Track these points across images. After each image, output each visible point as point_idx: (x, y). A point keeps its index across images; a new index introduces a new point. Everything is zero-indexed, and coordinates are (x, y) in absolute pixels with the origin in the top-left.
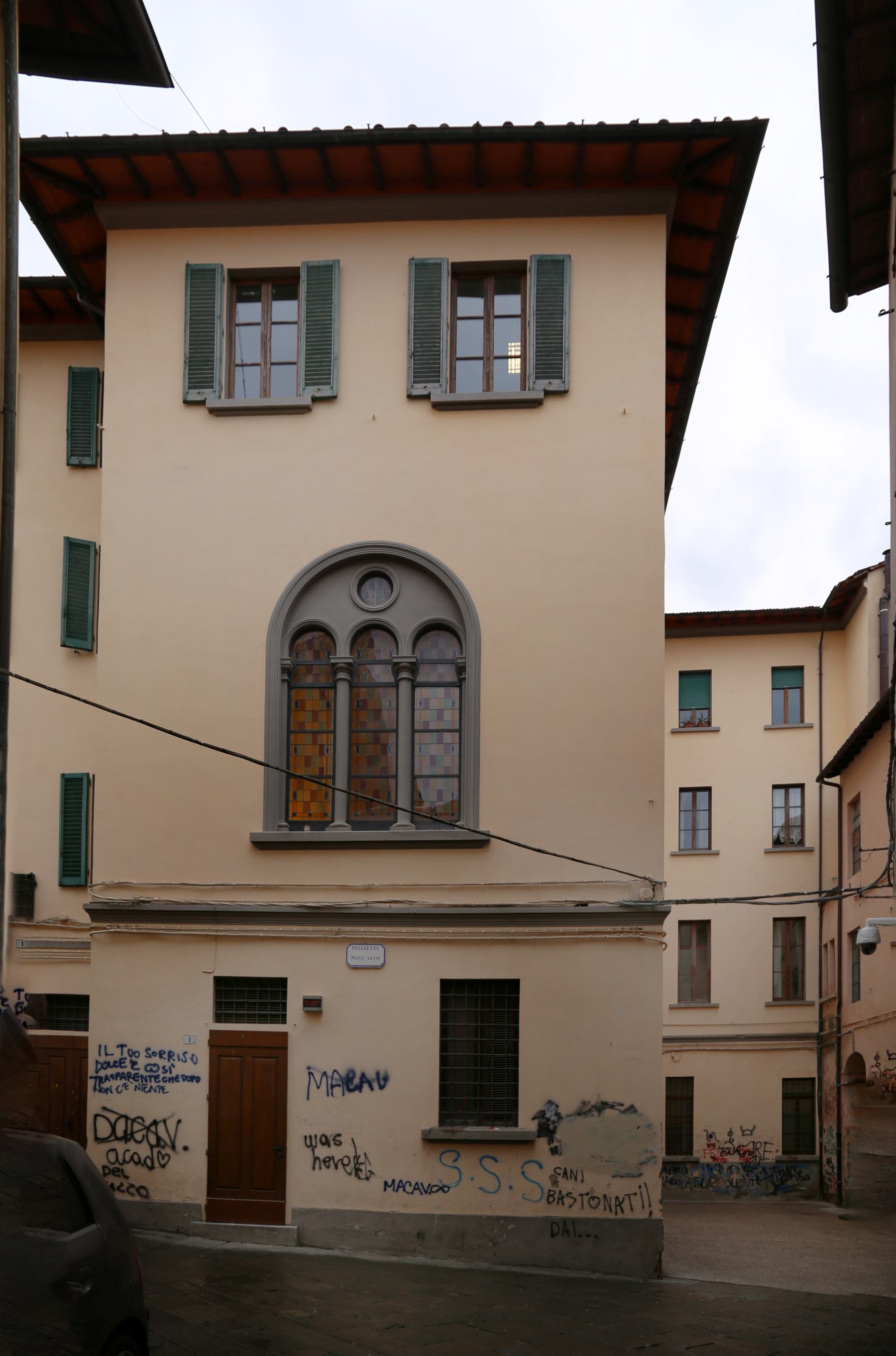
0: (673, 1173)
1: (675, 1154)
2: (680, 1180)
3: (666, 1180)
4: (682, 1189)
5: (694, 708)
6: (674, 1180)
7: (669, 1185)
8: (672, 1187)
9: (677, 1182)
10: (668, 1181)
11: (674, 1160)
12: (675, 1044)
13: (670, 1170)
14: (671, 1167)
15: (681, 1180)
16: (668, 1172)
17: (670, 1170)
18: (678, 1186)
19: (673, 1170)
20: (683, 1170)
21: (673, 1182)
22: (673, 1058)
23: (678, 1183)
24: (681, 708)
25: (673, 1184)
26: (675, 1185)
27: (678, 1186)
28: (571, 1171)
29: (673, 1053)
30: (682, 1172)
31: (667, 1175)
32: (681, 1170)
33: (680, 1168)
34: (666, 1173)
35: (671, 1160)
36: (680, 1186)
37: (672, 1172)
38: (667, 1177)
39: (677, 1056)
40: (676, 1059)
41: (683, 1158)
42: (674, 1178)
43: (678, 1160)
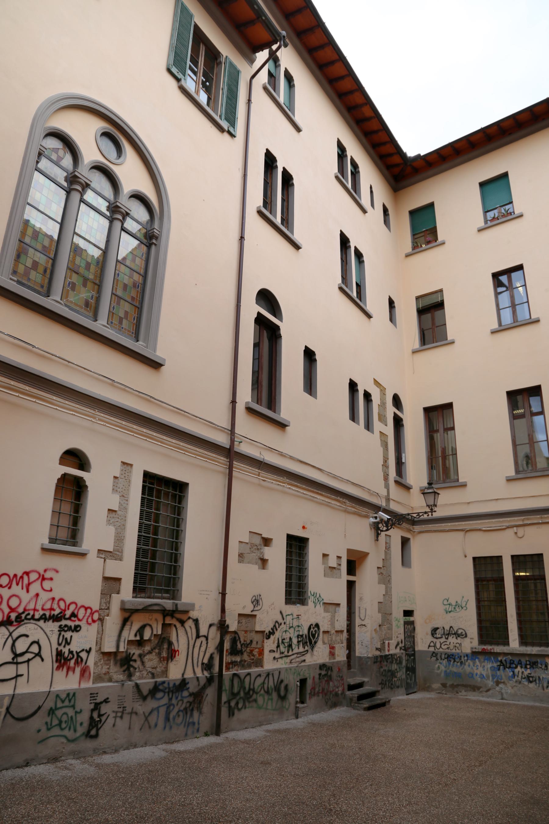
0: (530, 668)
1: (533, 645)
2: (539, 677)
3: (522, 676)
4: (544, 689)
5: (498, 206)
6: (532, 677)
7: (526, 683)
8: (532, 685)
9: (535, 681)
10: (524, 678)
11: (529, 653)
12: (516, 518)
13: (526, 665)
14: (526, 661)
15: (541, 678)
16: (524, 666)
17: (526, 665)
18: (538, 685)
19: (529, 664)
20: (541, 665)
21: (531, 679)
22: (516, 533)
23: (537, 682)
24: (486, 210)
25: (531, 682)
26: (534, 683)
27: (538, 685)
28: (118, 705)
29: (515, 528)
30: (541, 668)
31: (523, 670)
32: (539, 665)
33: (537, 662)
34: (521, 667)
35: (525, 653)
36: (541, 685)
37: (528, 667)
38: (523, 672)
39: (521, 531)
40: (520, 534)
41: (539, 651)
42: (532, 675)
43: (533, 653)
